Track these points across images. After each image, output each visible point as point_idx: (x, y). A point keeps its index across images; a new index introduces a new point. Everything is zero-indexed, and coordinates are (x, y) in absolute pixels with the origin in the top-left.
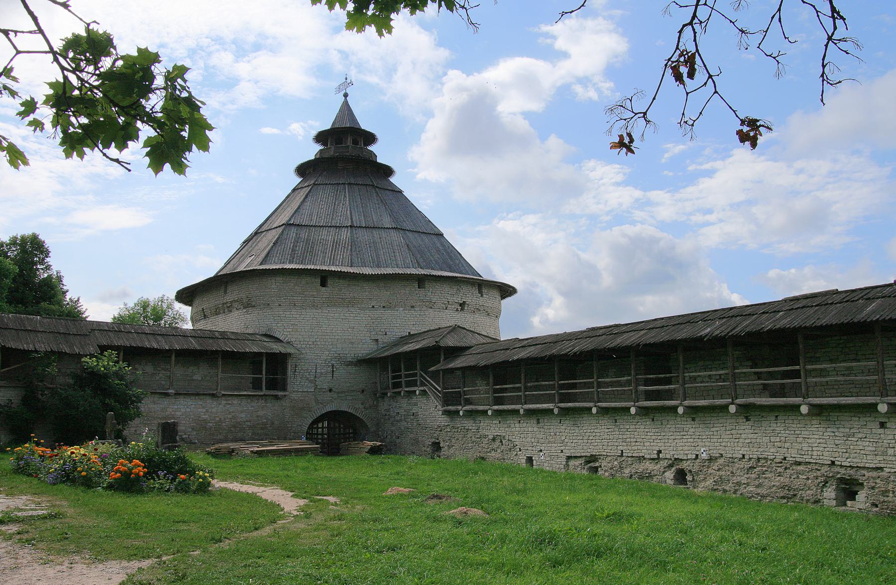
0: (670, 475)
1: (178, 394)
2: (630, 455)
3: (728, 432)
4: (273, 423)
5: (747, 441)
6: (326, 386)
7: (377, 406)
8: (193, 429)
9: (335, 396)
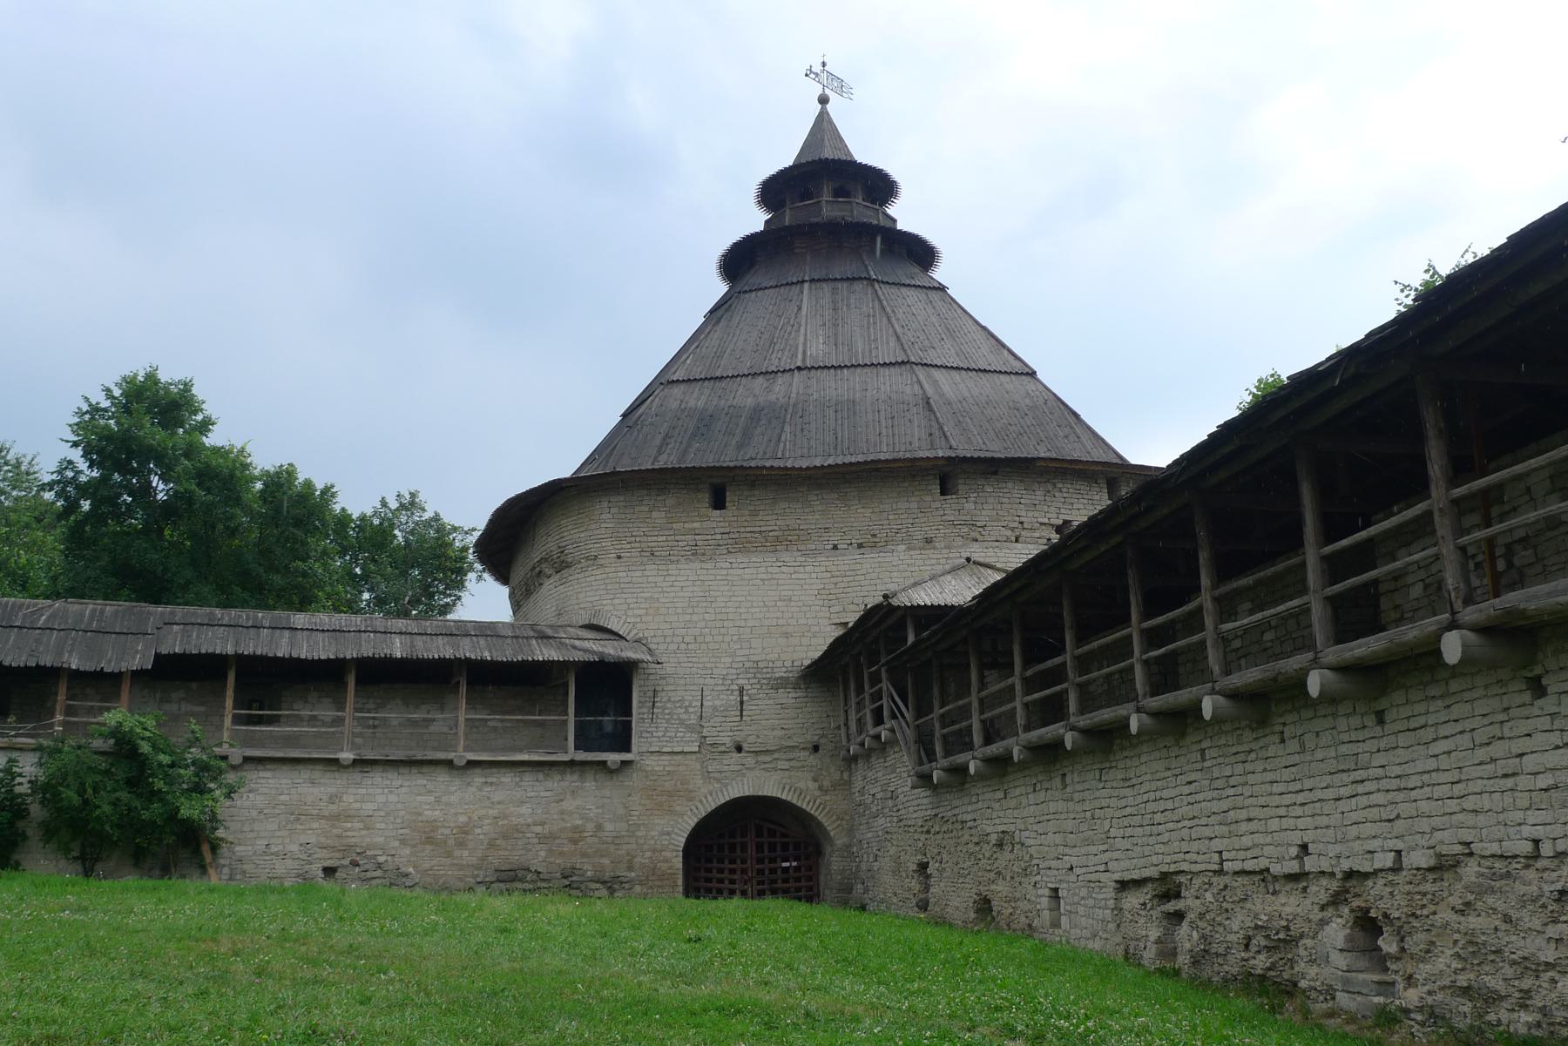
0: (1337, 931)
1: (361, 764)
2: (1238, 866)
3: (1481, 754)
4: (599, 827)
5: (1543, 781)
6: (726, 739)
7: (849, 783)
8: (403, 842)
9: (750, 760)
